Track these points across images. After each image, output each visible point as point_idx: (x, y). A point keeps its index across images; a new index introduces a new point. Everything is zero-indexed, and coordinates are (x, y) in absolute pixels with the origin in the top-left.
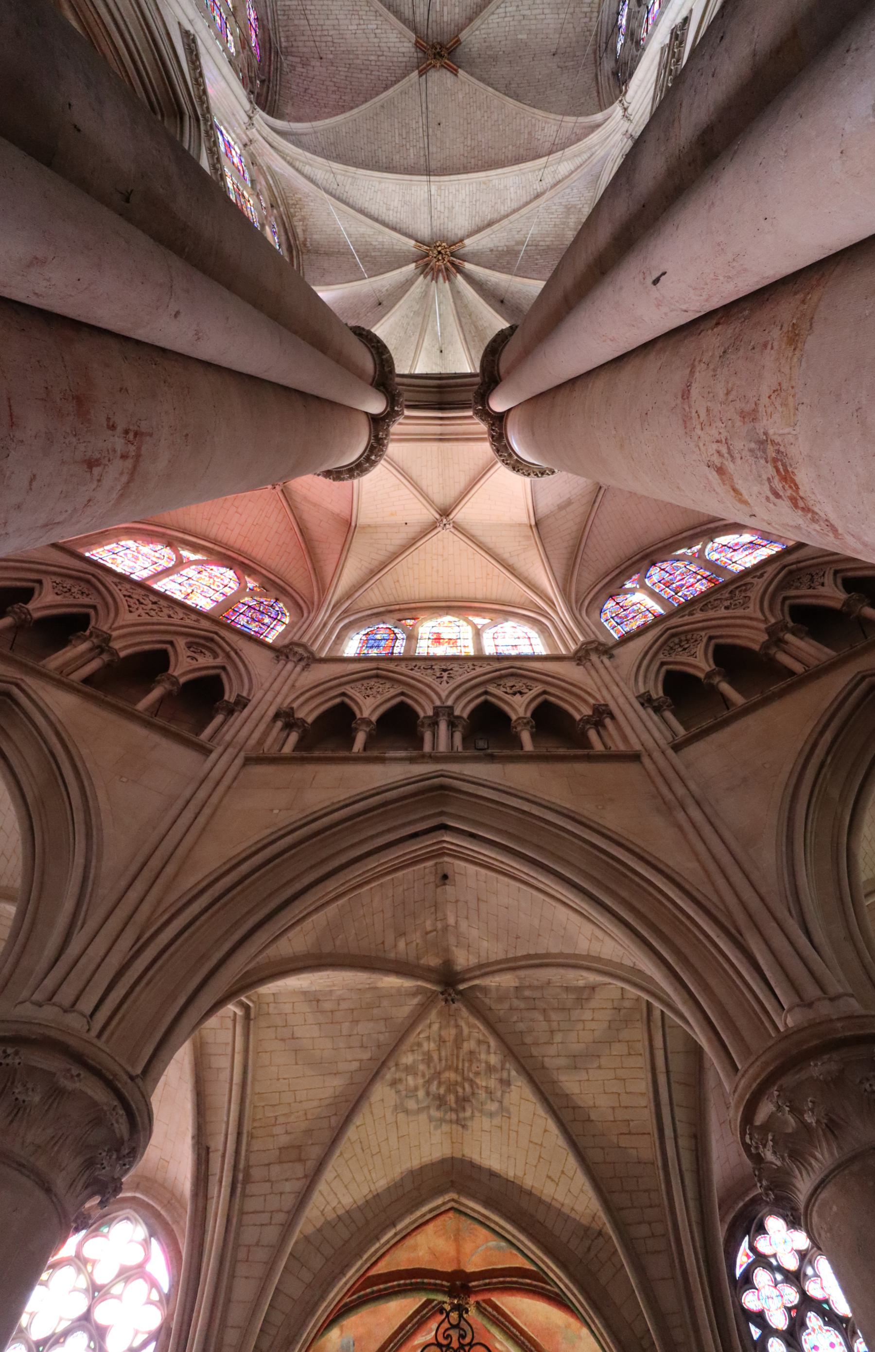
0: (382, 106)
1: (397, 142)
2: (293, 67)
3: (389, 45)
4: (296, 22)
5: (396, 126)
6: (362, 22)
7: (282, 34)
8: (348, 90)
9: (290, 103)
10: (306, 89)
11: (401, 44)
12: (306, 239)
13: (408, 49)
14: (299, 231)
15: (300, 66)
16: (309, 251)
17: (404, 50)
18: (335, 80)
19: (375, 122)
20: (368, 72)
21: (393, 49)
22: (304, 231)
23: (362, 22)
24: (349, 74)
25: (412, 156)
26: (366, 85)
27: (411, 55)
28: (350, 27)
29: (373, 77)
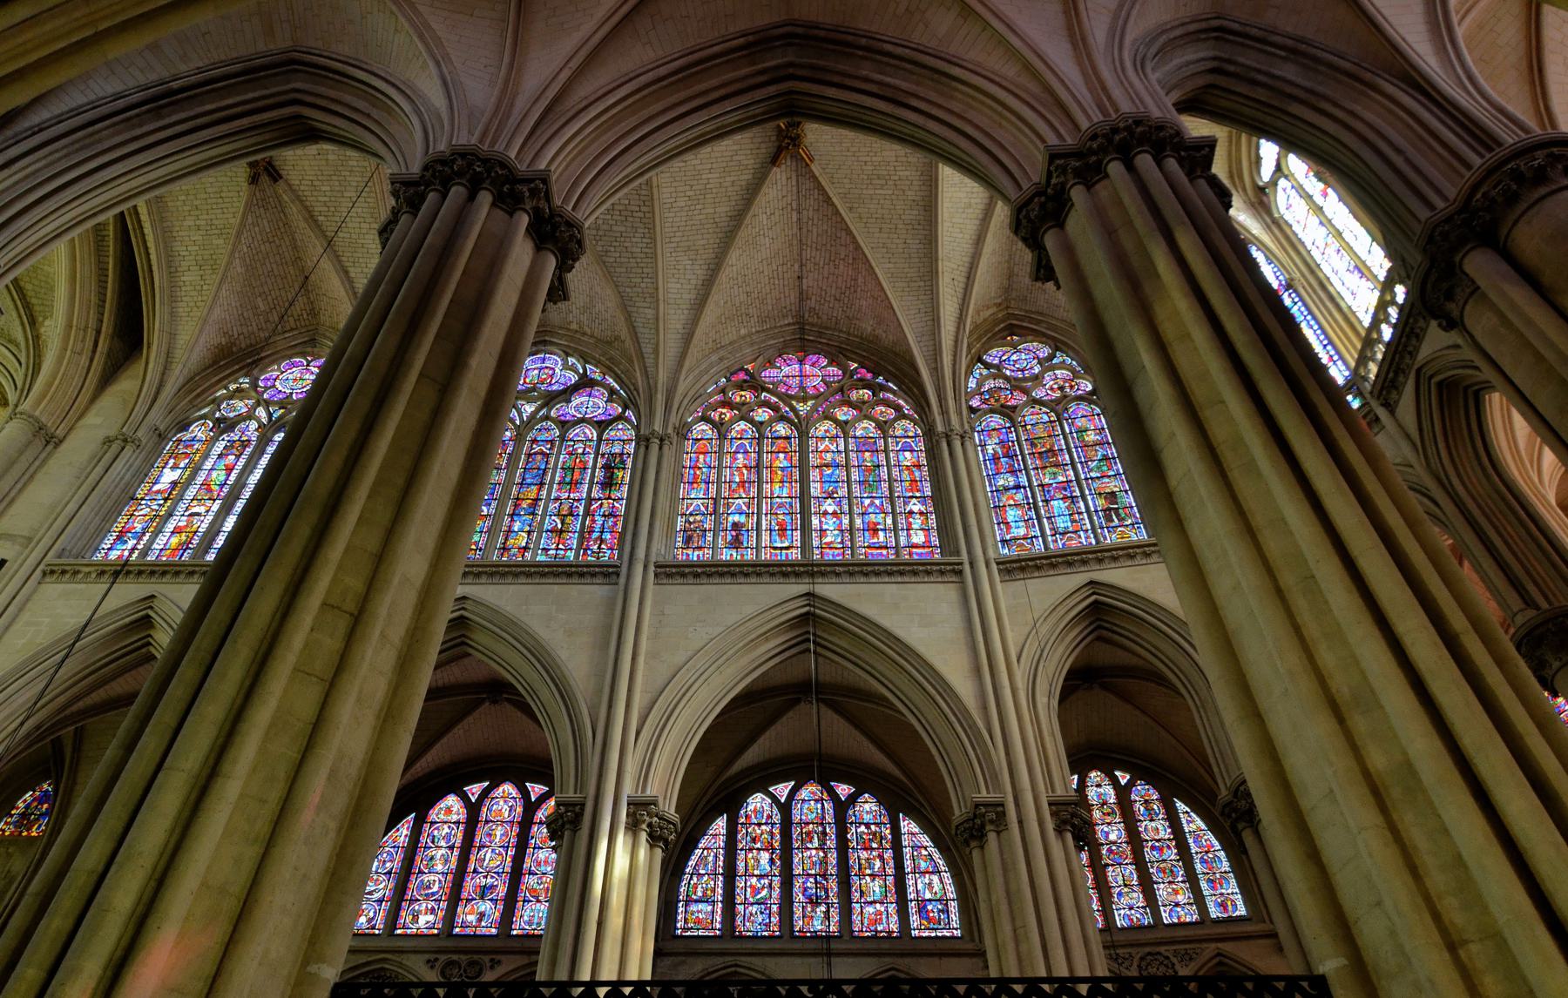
0: (851, 209)
1: (890, 192)
2: (812, 310)
3: (780, 197)
4: (770, 308)
5: (872, 192)
6: (762, 233)
7: (782, 323)
8: (833, 249)
9: (857, 322)
10: (836, 299)
11: (779, 184)
12: (995, 304)
13: (784, 174)
14: (988, 313)
15: (809, 302)
16: (1006, 299)
17: (784, 178)
18: (821, 265)
19: (869, 220)
20: (810, 223)
21: (785, 194)
22: (988, 308)
23: (762, 233)
24: (814, 245)
25: (908, 173)
26: (825, 227)
27: (789, 169)
28: (768, 246)
29: (815, 217)
